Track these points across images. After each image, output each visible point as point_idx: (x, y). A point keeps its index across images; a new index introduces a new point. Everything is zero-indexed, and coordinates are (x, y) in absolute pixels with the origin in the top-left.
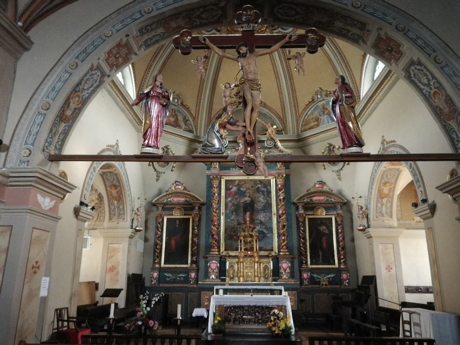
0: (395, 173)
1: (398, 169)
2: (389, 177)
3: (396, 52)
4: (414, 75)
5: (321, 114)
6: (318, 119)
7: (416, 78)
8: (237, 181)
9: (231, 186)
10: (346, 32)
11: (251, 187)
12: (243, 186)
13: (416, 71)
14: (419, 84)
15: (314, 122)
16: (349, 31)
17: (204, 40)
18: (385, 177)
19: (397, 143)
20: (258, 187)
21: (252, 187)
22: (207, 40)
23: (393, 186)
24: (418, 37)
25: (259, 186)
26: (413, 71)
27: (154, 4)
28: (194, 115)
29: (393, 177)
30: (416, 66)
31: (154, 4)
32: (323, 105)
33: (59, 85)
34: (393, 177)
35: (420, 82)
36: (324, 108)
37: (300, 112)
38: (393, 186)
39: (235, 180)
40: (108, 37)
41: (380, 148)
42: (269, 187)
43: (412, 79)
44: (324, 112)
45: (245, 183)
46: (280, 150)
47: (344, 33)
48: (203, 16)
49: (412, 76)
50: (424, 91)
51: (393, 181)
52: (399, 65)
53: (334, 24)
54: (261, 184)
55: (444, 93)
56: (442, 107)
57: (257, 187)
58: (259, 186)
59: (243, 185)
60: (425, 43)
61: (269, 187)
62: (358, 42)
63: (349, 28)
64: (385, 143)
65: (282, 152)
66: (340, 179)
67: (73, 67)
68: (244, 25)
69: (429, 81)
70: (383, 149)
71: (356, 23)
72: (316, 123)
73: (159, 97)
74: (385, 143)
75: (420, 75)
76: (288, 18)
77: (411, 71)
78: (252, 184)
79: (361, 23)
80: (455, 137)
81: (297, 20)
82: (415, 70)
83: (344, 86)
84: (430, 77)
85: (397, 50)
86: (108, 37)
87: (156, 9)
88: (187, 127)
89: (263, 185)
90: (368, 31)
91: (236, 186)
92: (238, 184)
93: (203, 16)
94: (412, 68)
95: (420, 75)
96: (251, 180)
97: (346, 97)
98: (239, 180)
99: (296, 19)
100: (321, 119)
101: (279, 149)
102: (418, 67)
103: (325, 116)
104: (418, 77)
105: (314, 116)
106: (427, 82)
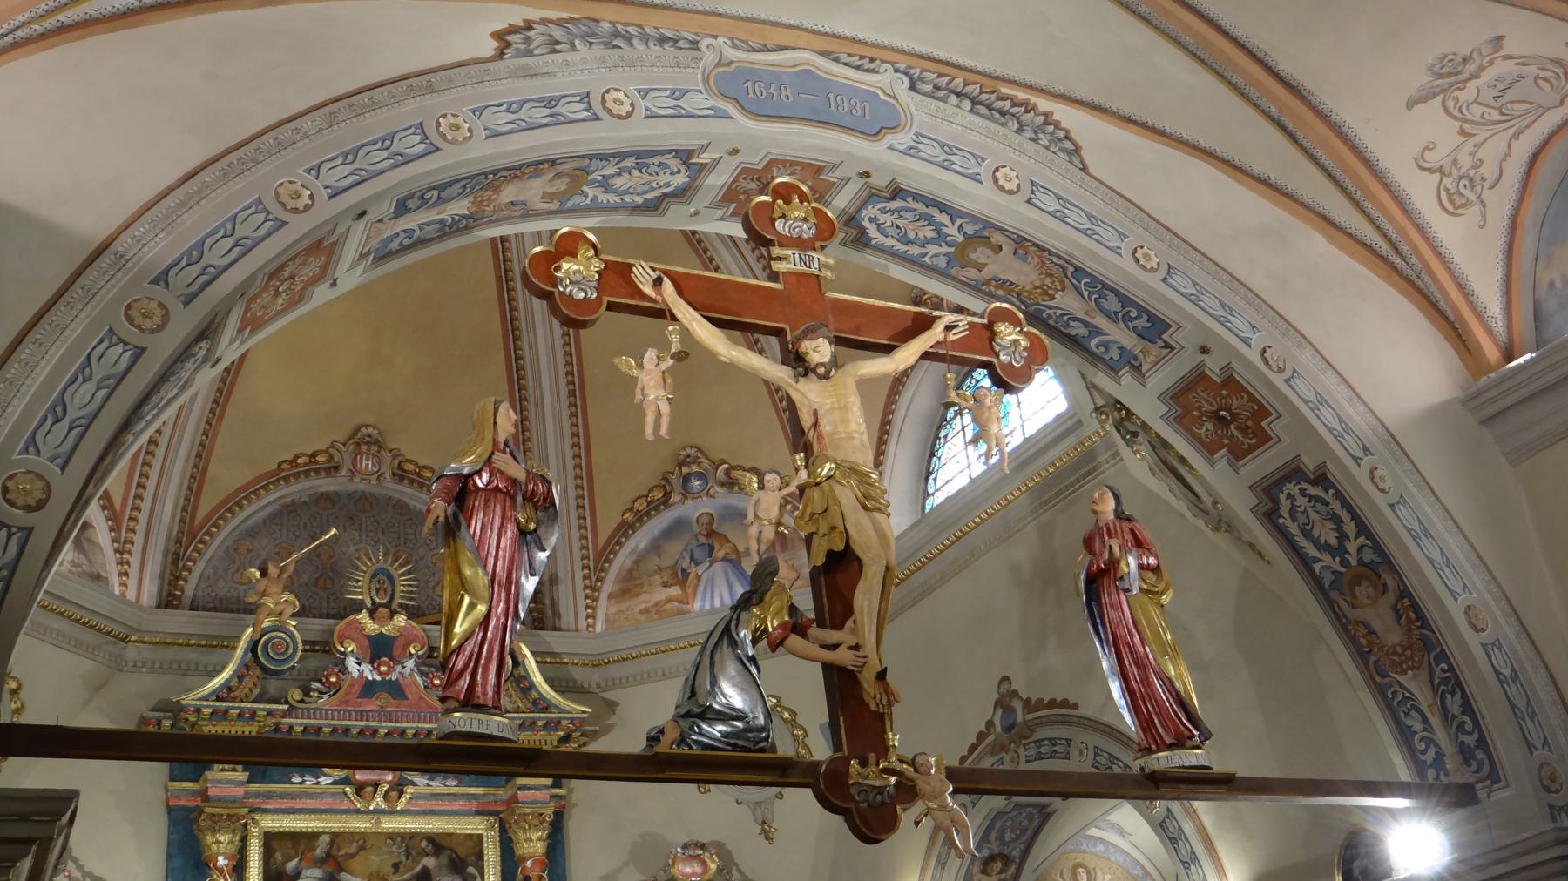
0: (1031, 820)
1: (1044, 807)
2: (1007, 837)
3: (1244, 430)
4: (1292, 512)
5: (698, 553)
6: (685, 573)
7: (1294, 519)
8: (325, 839)
9: (291, 865)
10: (1083, 331)
11: (389, 869)
12: (355, 864)
13: (1302, 502)
14: (1302, 542)
15: (666, 585)
16: (1095, 331)
17: (658, 283)
18: (993, 835)
19: (1081, 712)
20: (425, 871)
21: (396, 867)
22: (668, 286)
23: (1012, 870)
24: (1322, 401)
25: (429, 862)
26: (1289, 496)
27: (474, 111)
28: (118, 506)
29: (1018, 837)
30: (1305, 485)
31: (474, 111)
32: (705, 520)
33: (83, 396)
34: (1018, 837)
35: (1307, 534)
36: (711, 533)
37: (602, 541)
38: (1012, 870)
39: (313, 836)
40: (295, 210)
41: (990, 724)
42: (471, 870)
43: (1281, 521)
44: (711, 549)
45: (362, 848)
46: (535, 703)
47: (1073, 332)
48: (618, 182)
49: (1284, 511)
50: (1317, 567)
51: (1016, 853)
52: (1243, 471)
53: (1052, 298)
54: (436, 854)
55: (1391, 583)
56: (1376, 625)
57: (418, 868)
58: (429, 862)
59: (352, 856)
60: (1341, 421)
61: (471, 870)
62: (1116, 372)
63: (1100, 321)
64: (1018, 706)
65: (546, 709)
66: (767, 836)
67: (148, 324)
68: (789, 252)
69: (1343, 537)
70: (1009, 728)
71: (1134, 314)
72: (675, 591)
73: (513, 498)
74: (1018, 706)
75: (1313, 516)
76: (902, 248)
77: (1282, 497)
78: (397, 852)
79: (1151, 317)
80: (1418, 726)
81: (927, 259)
82: (1298, 497)
83: (1126, 525)
84: (1350, 528)
85: (1249, 423)
86: (295, 210)
87: (484, 134)
88: (83, 559)
89: (444, 859)
90: (1167, 345)
91: (321, 862)
92: (328, 857)
93: (618, 182)
94: (1291, 488)
95: (1313, 516)
96: (392, 836)
97: (1141, 567)
98: (335, 836)
99: (925, 255)
100: (699, 577)
101: (534, 694)
102: (1314, 491)
103: (718, 566)
104: (1302, 519)
105: (667, 561)
106: (1333, 542)
